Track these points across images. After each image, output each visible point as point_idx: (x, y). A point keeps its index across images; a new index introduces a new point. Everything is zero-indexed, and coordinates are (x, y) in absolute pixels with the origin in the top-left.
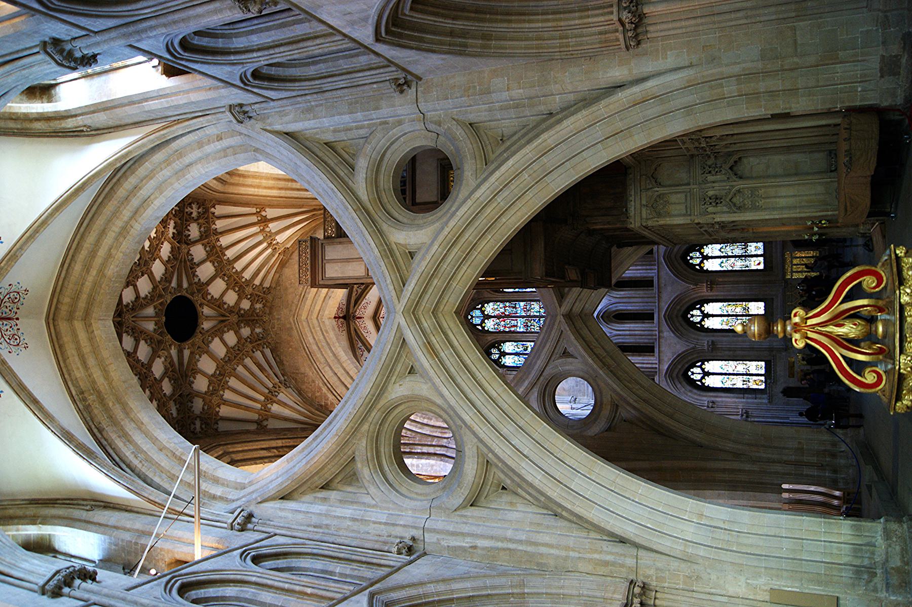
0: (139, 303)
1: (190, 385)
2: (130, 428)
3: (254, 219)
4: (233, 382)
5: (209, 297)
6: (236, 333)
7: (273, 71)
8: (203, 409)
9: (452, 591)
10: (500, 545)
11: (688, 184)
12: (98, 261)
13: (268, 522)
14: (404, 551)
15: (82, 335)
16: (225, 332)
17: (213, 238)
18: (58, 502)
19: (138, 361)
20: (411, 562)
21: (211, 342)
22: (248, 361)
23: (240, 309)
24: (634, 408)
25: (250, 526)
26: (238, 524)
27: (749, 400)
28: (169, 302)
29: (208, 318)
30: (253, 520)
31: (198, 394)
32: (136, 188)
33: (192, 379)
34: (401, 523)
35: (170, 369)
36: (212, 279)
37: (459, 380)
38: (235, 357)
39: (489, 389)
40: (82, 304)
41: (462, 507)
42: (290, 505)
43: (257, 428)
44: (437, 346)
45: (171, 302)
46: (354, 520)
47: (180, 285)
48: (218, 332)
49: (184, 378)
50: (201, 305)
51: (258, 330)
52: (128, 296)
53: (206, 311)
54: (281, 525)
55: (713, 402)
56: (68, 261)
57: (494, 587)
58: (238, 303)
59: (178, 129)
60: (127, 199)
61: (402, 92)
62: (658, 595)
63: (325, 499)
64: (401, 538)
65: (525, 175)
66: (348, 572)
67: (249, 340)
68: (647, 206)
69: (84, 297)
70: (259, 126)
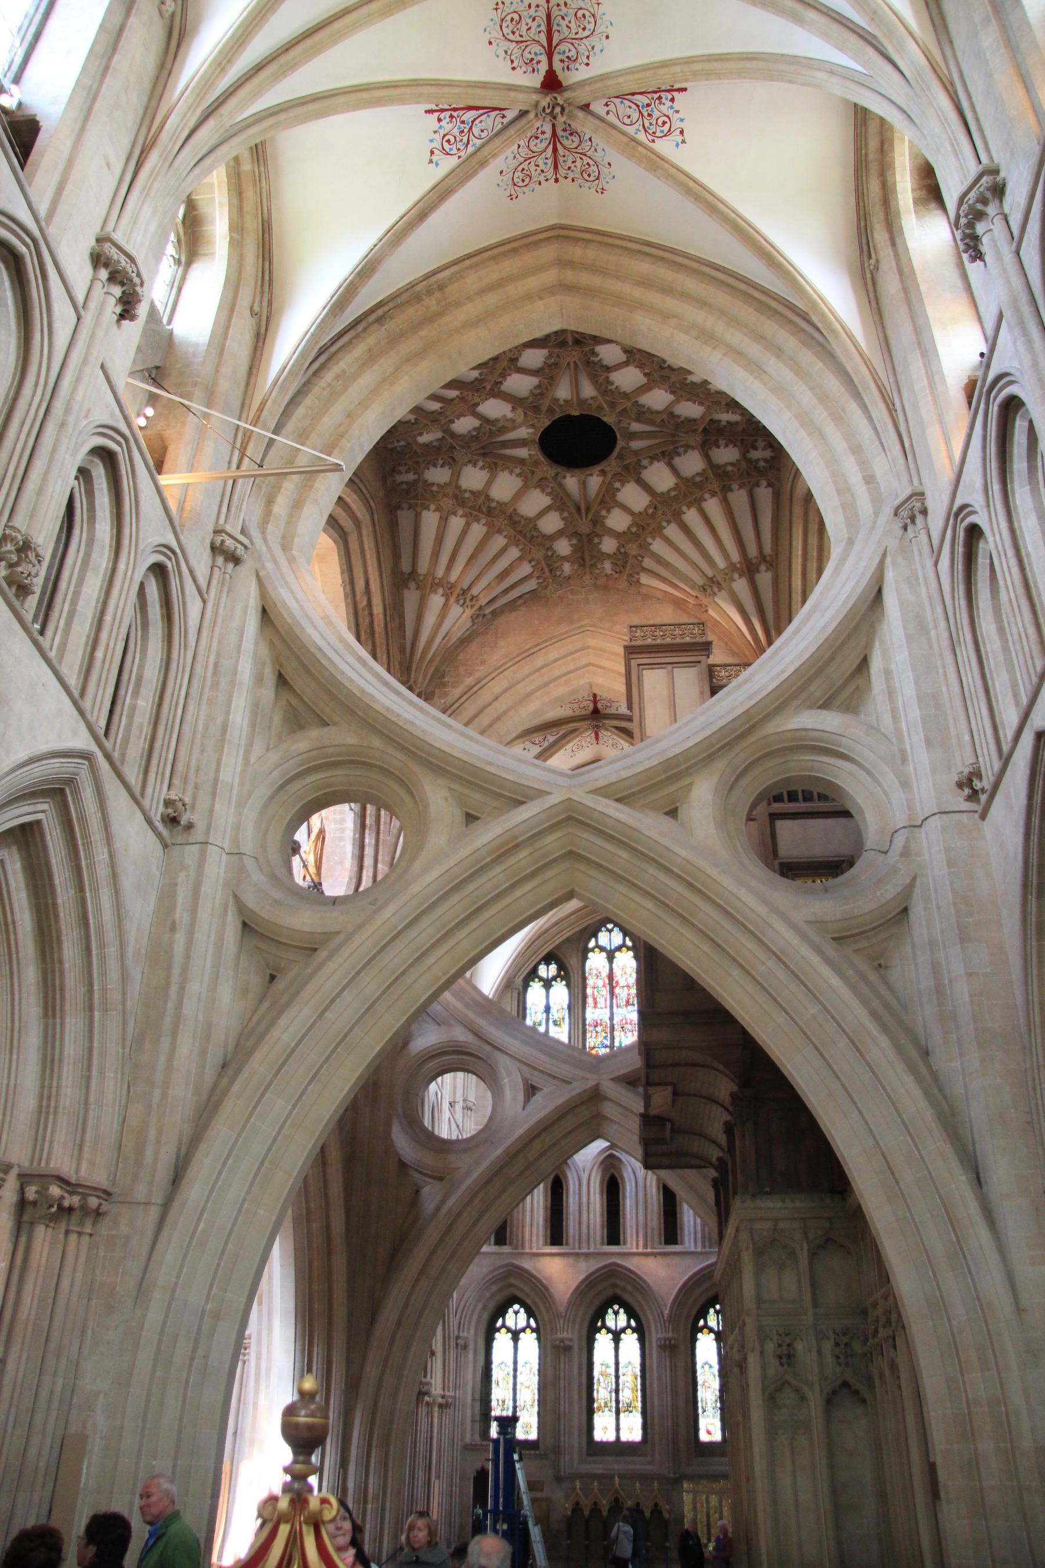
0: (599, 372)
1: (470, 461)
2: (386, 364)
3: (753, 551)
4: (478, 530)
5: (617, 485)
6: (560, 533)
7: (982, 562)
8: (433, 484)
9: (96, 890)
10: (176, 970)
11: (815, 1304)
12: (656, 299)
13: (226, 589)
14: (170, 811)
15: (533, 282)
16: (561, 514)
17: (716, 486)
18: (267, 264)
19: (504, 375)
20: (149, 822)
21: (543, 491)
22: (514, 553)
23: (600, 536)
24: (438, 1208)
25: (220, 560)
26: (223, 542)
27: (469, 1410)
28: (605, 419)
29: (583, 484)
30: (230, 566)
31: (456, 475)
32: (778, 352)
33: (480, 464)
34: (217, 806)
35: (494, 428)
37: (454, 899)
38: (520, 532)
39: (439, 952)
40: (585, 279)
41: (241, 908)
42: (252, 624)
43: (402, 574)
44: (512, 861)
45: (604, 424)
46: (225, 728)
47: (634, 436)
48: (561, 502)
49: (482, 451)
50: (603, 472)
51: (567, 568)
52: (609, 354)
53: (595, 481)
54: (221, 611)
55: (465, 1347)
56: (653, 251)
57: (102, 958)
58: (611, 532)
59: (879, 412)
60: (759, 338)
61: (960, 785)
62: (85, 1240)
63: (259, 680)
64: (193, 807)
65: (813, 1010)
66: (137, 720)
68: (775, 1229)
69: (597, 281)
70: (892, 543)
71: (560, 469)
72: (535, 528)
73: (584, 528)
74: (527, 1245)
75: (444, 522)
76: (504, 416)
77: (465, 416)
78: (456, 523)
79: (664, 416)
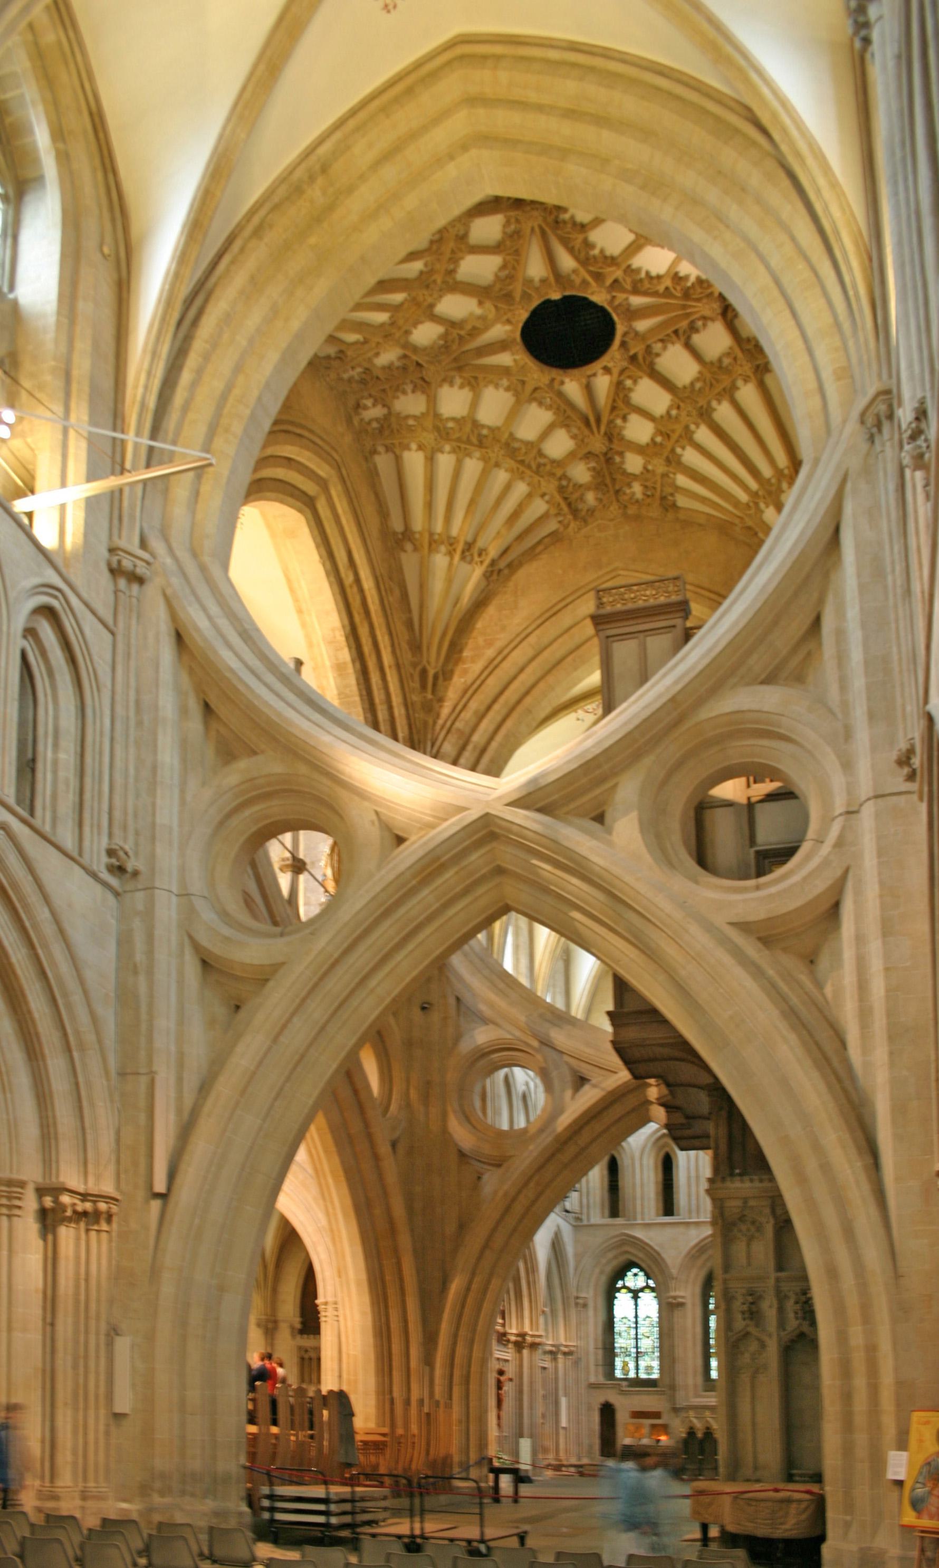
1: (444, 380)
8: (407, 417)
16: (569, 431)
19: (455, 260)
21: (540, 404)
22: (521, 488)
31: (432, 401)
33: (458, 381)
35: (462, 333)
36: (665, 383)
38: (522, 462)
47: (633, 314)
49: (455, 365)
50: (607, 370)
53: (603, 384)
67: (564, 483)
71: (555, 373)
72: (540, 454)
73: (597, 444)
74: (639, 1216)
75: (431, 460)
76: (471, 314)
77: (421, 322)
78: (445, 461)
79: (668, 282)
